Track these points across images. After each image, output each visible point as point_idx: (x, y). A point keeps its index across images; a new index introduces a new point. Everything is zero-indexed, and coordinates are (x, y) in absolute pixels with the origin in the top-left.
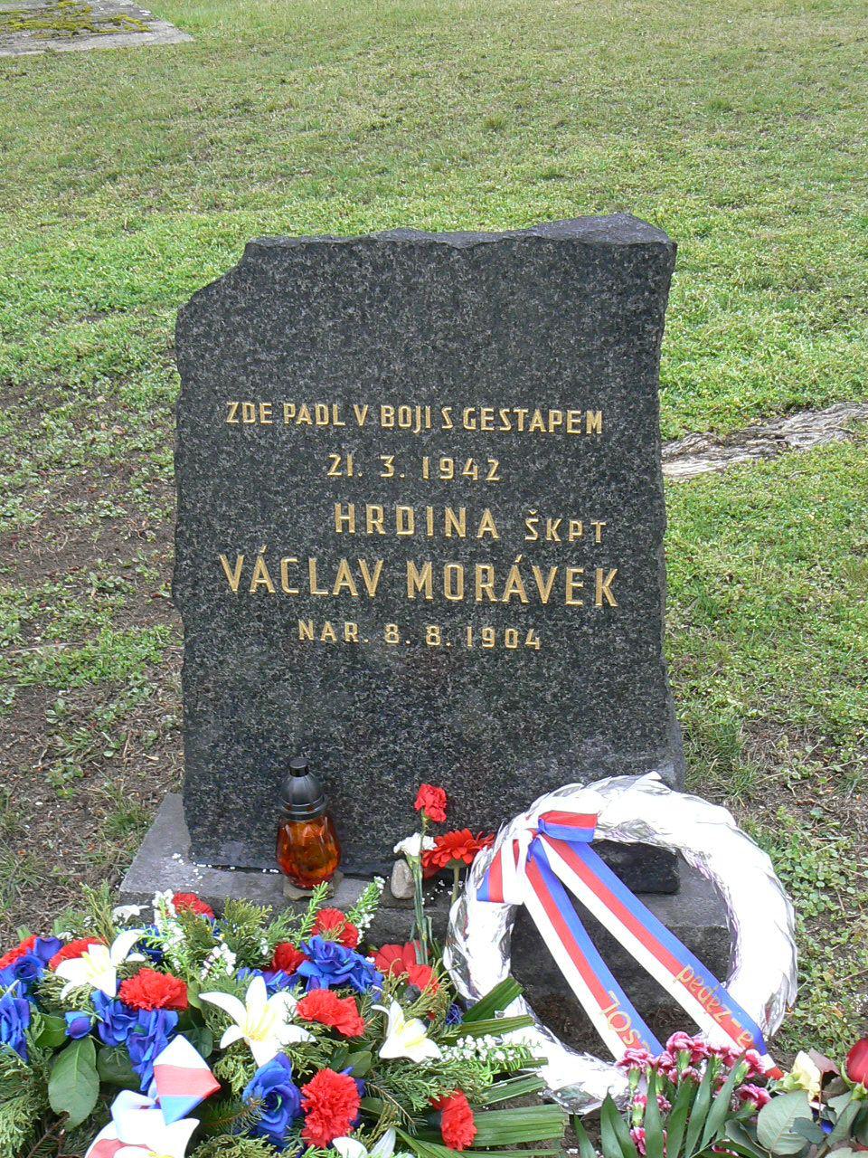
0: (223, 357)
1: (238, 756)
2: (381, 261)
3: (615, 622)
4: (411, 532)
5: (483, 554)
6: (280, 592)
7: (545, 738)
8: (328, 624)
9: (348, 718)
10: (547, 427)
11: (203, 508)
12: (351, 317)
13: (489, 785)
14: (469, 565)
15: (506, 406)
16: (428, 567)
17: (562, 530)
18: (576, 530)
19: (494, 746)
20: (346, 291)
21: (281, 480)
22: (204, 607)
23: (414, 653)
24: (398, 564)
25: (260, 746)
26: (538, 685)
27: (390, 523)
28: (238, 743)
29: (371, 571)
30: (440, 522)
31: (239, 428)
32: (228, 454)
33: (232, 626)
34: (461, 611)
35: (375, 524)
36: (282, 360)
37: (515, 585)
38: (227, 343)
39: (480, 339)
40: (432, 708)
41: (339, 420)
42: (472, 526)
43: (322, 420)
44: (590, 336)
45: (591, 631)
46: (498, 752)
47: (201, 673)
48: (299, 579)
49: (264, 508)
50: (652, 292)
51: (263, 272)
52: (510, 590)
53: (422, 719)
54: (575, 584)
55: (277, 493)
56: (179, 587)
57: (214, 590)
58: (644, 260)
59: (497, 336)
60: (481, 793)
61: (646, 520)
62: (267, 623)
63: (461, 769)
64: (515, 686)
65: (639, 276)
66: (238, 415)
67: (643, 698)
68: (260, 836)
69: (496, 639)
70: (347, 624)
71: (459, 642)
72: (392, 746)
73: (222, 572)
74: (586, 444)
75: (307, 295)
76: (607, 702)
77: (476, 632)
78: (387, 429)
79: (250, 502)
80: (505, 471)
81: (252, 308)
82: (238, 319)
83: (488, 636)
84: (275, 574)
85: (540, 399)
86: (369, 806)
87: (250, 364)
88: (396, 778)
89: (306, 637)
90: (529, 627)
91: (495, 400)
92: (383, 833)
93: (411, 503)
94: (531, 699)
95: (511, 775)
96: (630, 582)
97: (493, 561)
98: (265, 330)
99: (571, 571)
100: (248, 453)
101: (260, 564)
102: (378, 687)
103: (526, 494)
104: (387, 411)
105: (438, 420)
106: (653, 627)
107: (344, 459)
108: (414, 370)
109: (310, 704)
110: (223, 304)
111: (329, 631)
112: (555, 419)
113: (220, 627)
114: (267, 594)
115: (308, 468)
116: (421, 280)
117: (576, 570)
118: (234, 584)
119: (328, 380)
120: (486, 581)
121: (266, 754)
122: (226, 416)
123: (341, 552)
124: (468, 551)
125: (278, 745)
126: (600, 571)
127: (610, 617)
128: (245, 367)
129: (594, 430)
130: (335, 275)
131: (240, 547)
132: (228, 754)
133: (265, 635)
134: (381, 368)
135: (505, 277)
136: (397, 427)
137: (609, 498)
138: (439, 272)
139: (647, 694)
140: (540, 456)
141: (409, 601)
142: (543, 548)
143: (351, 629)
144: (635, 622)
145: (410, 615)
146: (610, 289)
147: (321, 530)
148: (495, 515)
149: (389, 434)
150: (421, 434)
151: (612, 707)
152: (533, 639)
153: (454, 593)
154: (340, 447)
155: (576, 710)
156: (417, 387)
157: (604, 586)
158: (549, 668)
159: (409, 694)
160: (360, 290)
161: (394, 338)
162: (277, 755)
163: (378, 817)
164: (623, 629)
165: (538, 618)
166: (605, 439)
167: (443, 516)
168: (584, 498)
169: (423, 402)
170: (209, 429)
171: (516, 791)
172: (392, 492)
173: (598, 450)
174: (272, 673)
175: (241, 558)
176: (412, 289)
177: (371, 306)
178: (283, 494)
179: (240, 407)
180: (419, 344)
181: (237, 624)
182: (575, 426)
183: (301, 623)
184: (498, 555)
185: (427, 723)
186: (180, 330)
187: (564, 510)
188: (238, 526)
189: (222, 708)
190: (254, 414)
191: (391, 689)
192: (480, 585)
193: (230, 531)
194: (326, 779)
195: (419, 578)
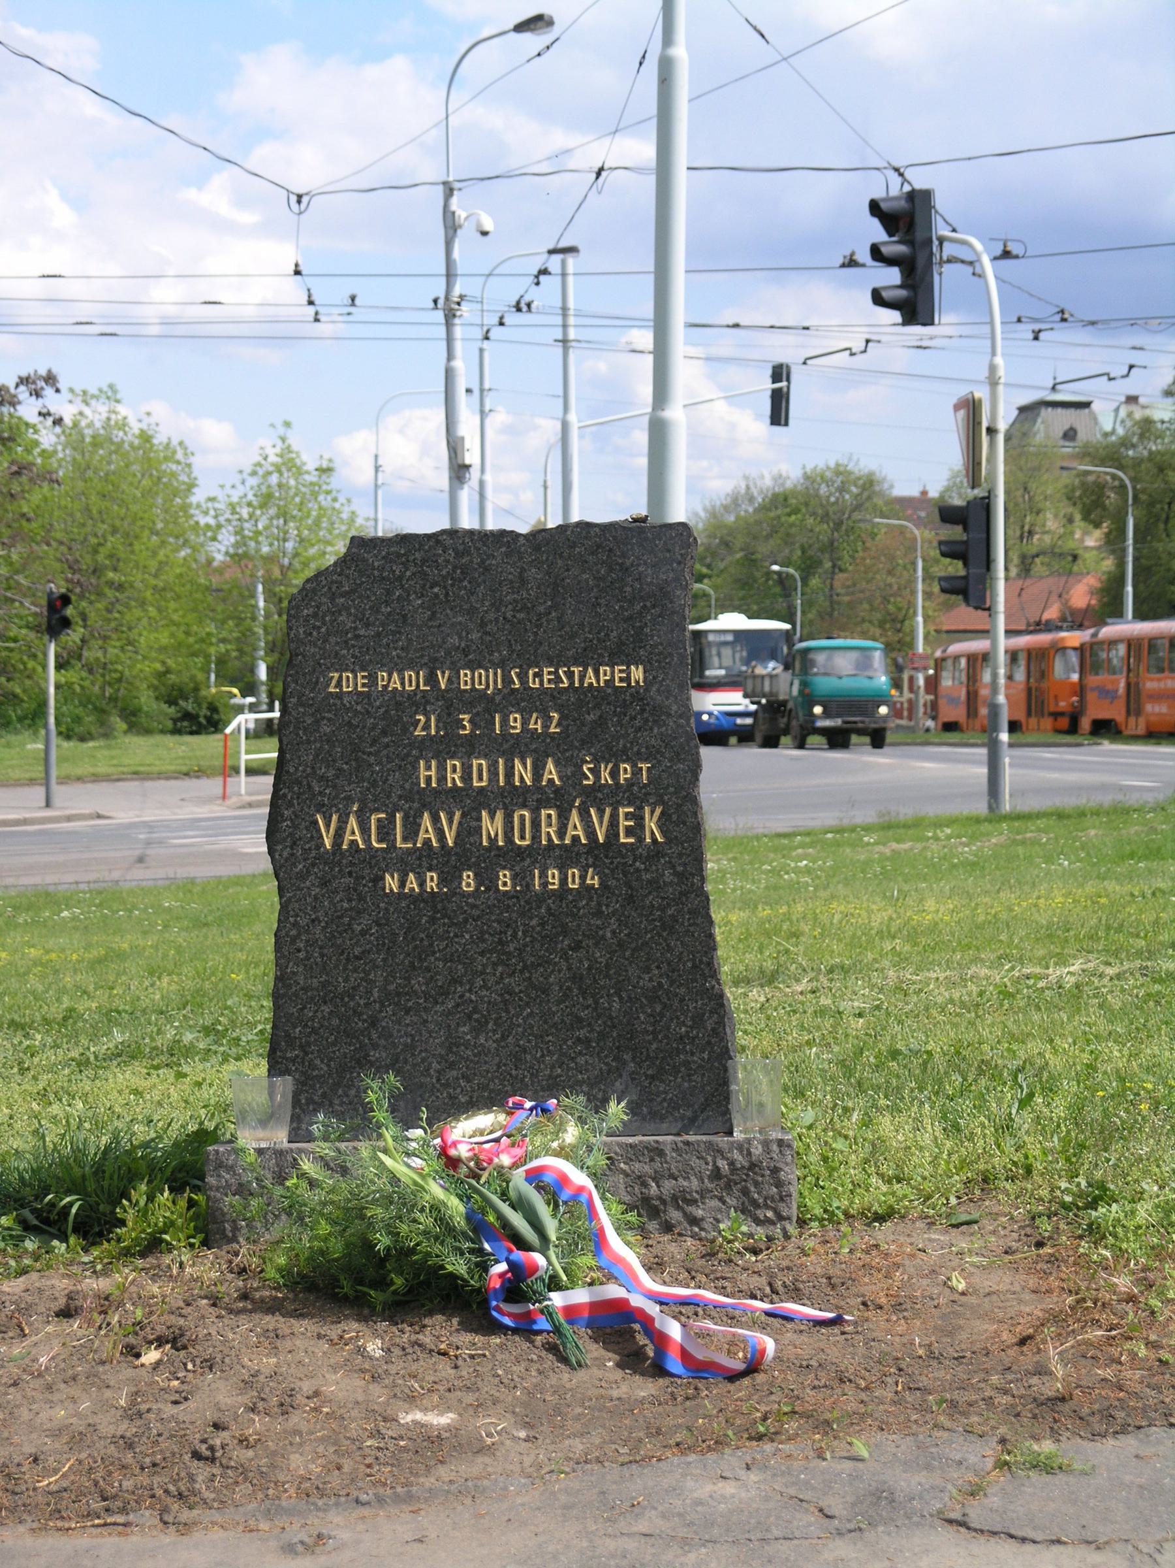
0: (328, 633)
1: (323, 1017)
2: (461, 548)
3: (663, 857)
4: (484, 784)
5: (548, 800)
6: (369, 846)
7: (607, 976)
8: (411, 876)
9: (428, 969)
10: (598, 681)
11: (304, 771)
12: (436, 595)
13: (557, 1029)
14: (535, 812)
15: (565, 666)
16: (499, 816)
17: (614, 774)
18: (626, 772)
19: (561, 988)
20: (433, 573)
21: (374, 742)
22: (301, 866)
23: (488, 898)
24: (474, 814)
25: (345, 1005)
26: (599, 922)
27: (467, 776)
28: (325, 1003)
29: (450, 822)
30: (509, 773)
31: (340, 696)
32: (329, 720)
33: (324, 883)
34: (529, 855)
35: (454, 778)
36: (378, 634)
37: (576, 828)
38: (332, 622)
39: (542, 609)
40: (505, 953)
41: (425, 685)
42: (537, 774)
43: (411, 685)
44: (631, 602)
45: (643, 867)
46: (565, 995)
47: (294, 932)
48: (387, 833)
49: (357, 769)
50: (679, 563)
51: (364, 560)
52: (570, 832)
53: (495, 964)
54: (627, 823)
55: (370, 754)
56: (279, 847)
57: (310, 849)
58: (672, 538)
59: (555, 607)
60: (550, 1038)
61: (685, 760)
62: (357, 878)
63: (531, 1014)
64: (579, 926)
65: (669, 551)
66: (339, 684)
67: (692, 929)
68: (341, 1105)
69: (560, 880)
70: (429, 874)
71: (528, 886)
72: (468, 995)
73: (319, 830)
74: (632, 695)
75: (400, 578)
76: (660, 936)
77: (543, 875)
78: (465, 691)
79: (346, 763)
80: (565, 723)
81: (353, 591)
82: (342, 600)
83: (553, 877)
84: (365, 830)
85: (592, 658)
86: (446, 1061)
87: (351, 639)
88: (473, 1029)
89: (391, 890)
90: (588, 866)
91: (556, 661)
92: (459, 1090)
93: (485, 757)
94: (594, 938)
95: (577, 1017)
96: (674, 817)
97: (558, 807)
98: (364, 609)
99: (622, 811)
100: (346, 718)
101: (353, 822)
102: (456, 936)
103: (583, 742)
104: (465, 675)
105: (507, 681)
106: (696, 860)
107: (428, 720)
108: (489, 638)
109: (394, 956)
110: (330, 588)
111: (412, 882)
112: (605, 675)
113: (313, 885)
114: (358, 850)
115: (398, 729)
116: (494, 562)
117: (627, 810)
118: (328, 843)
119: (416, 650)
120: (550, 825)
121: (351, 1012)
122: (328, 686)
123: (424, 806)
124: (535, 797)
125: (362, 1002)
126: (647, 810)
127: (658, 852)
128: (346, 642)
129: (637, 682)
130: (424, 561)
131: (335, 806)
132: (314, 1016)
133: (355, 890)
134: (460, 638)
135: (561, 556)
136: (473, 689)
137: (653, 742)
138: (508, 555)
139: (695, 924)
140: (594, 708)
141: (485, 848)
142: (599, 791)
143: (432, 879)
144: (680, 855)
145: (485, 862)
146: (645, 563)
147: (407, 786)
148: (557, 764)
149: (467, 695)
150: (493, 693)
151: (665, 940)
152: (593, 878)
153: (522, 838)
154: (425, 709)
155: (633, 945)
156: (491, 653)
157: (651, 824)
158: (607, 906)
159: (484, 941)
160: (444, 572)
161: (472, 611)
162: (361, 1014)
163: (454, 1073)
164: (670, 862)
165: (596, 857)
166: (647, 690)
167: (513, 767)
168: (632, 743)
169: (495, 666)
170: (313, 699)
171: (582, 1033)
172: (470, 747)
173: (642, 699)
174: (359, 928)
175: (335, 818)
176: (487, 569)
177: (452, 585)
178: (376, 754)
179: (341, 677)
180: (492, 616)
181: (329, 881)
182: (621, 680)
183: (388, 877)
184: (560, 799)
185: (500, 969)
186: (292, 612)
187: (614, 755)
188: (334, 787)
189: (311, 968)
190: (352, 682)
191: (467, 936)
192: (544, 829)
193: (327, 791)
194: (406, 1034)
195: (491, 826)
